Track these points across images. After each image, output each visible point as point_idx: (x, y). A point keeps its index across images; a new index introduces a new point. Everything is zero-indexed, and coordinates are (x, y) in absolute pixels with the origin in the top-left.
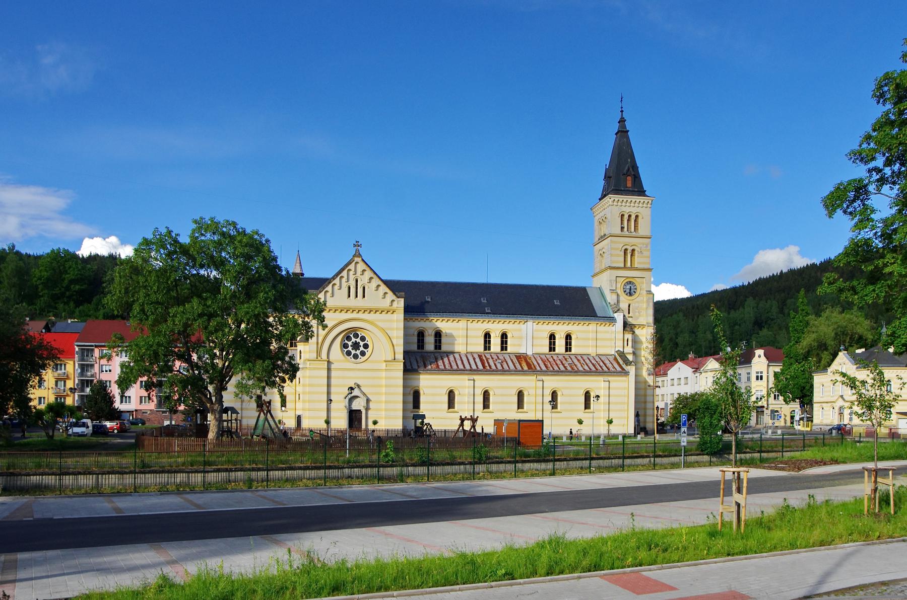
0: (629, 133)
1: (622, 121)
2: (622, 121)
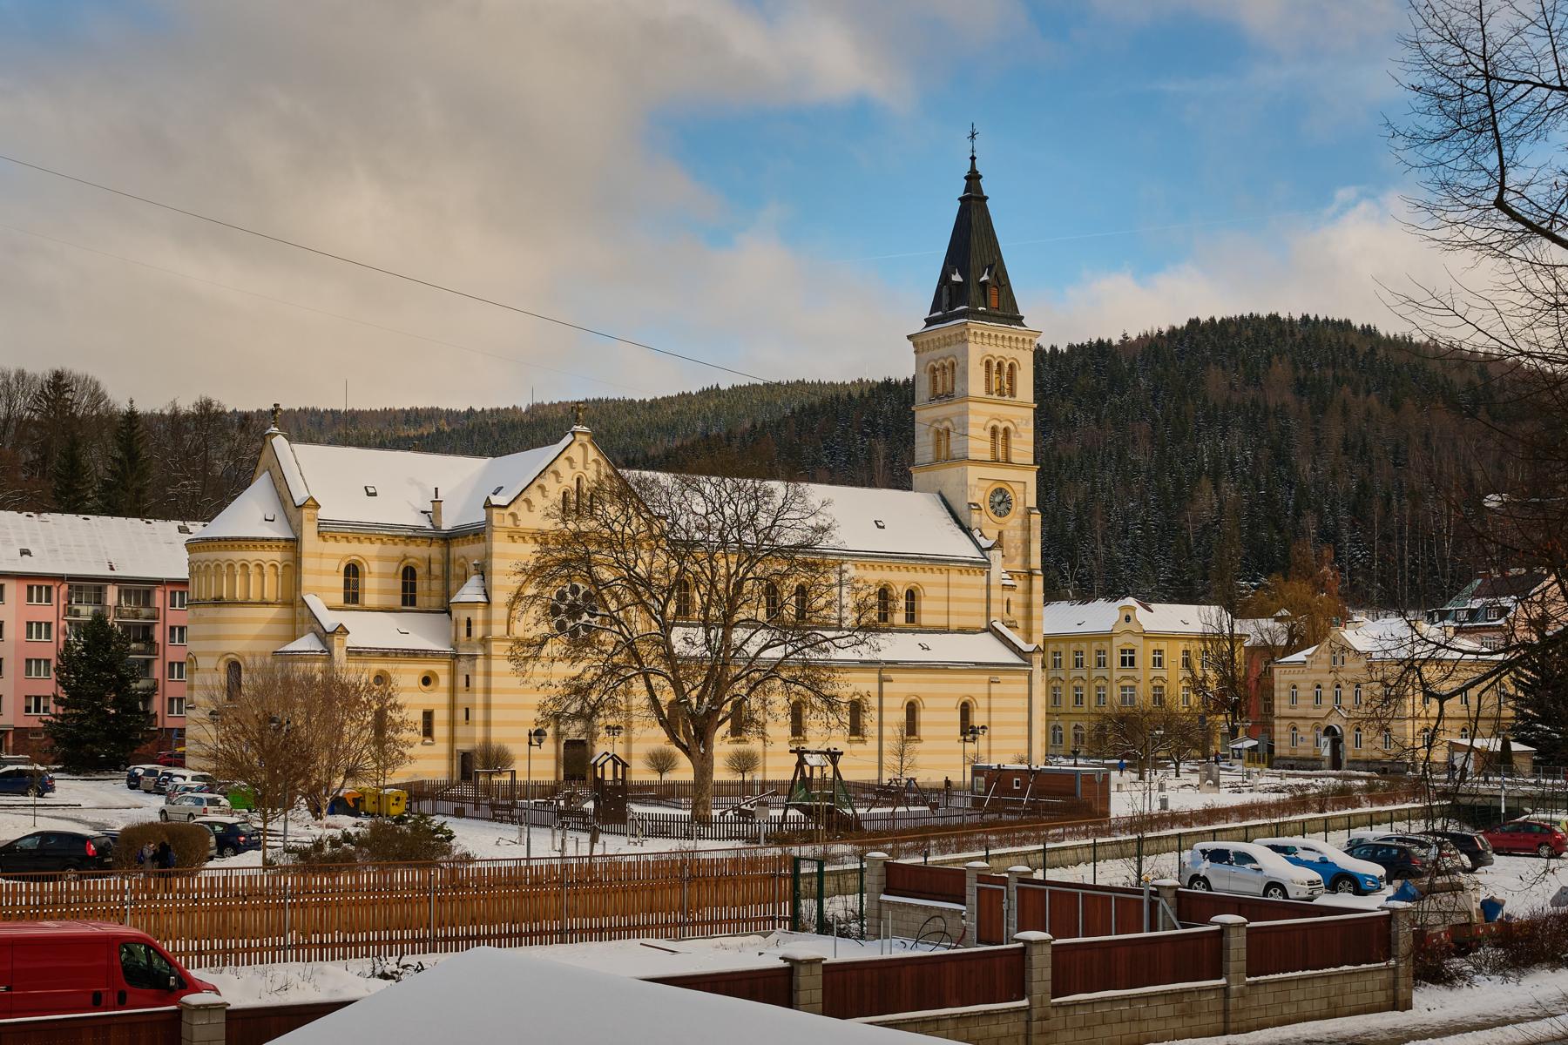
0: (988, 202)
1: (973, 178)
2: (973, 178)
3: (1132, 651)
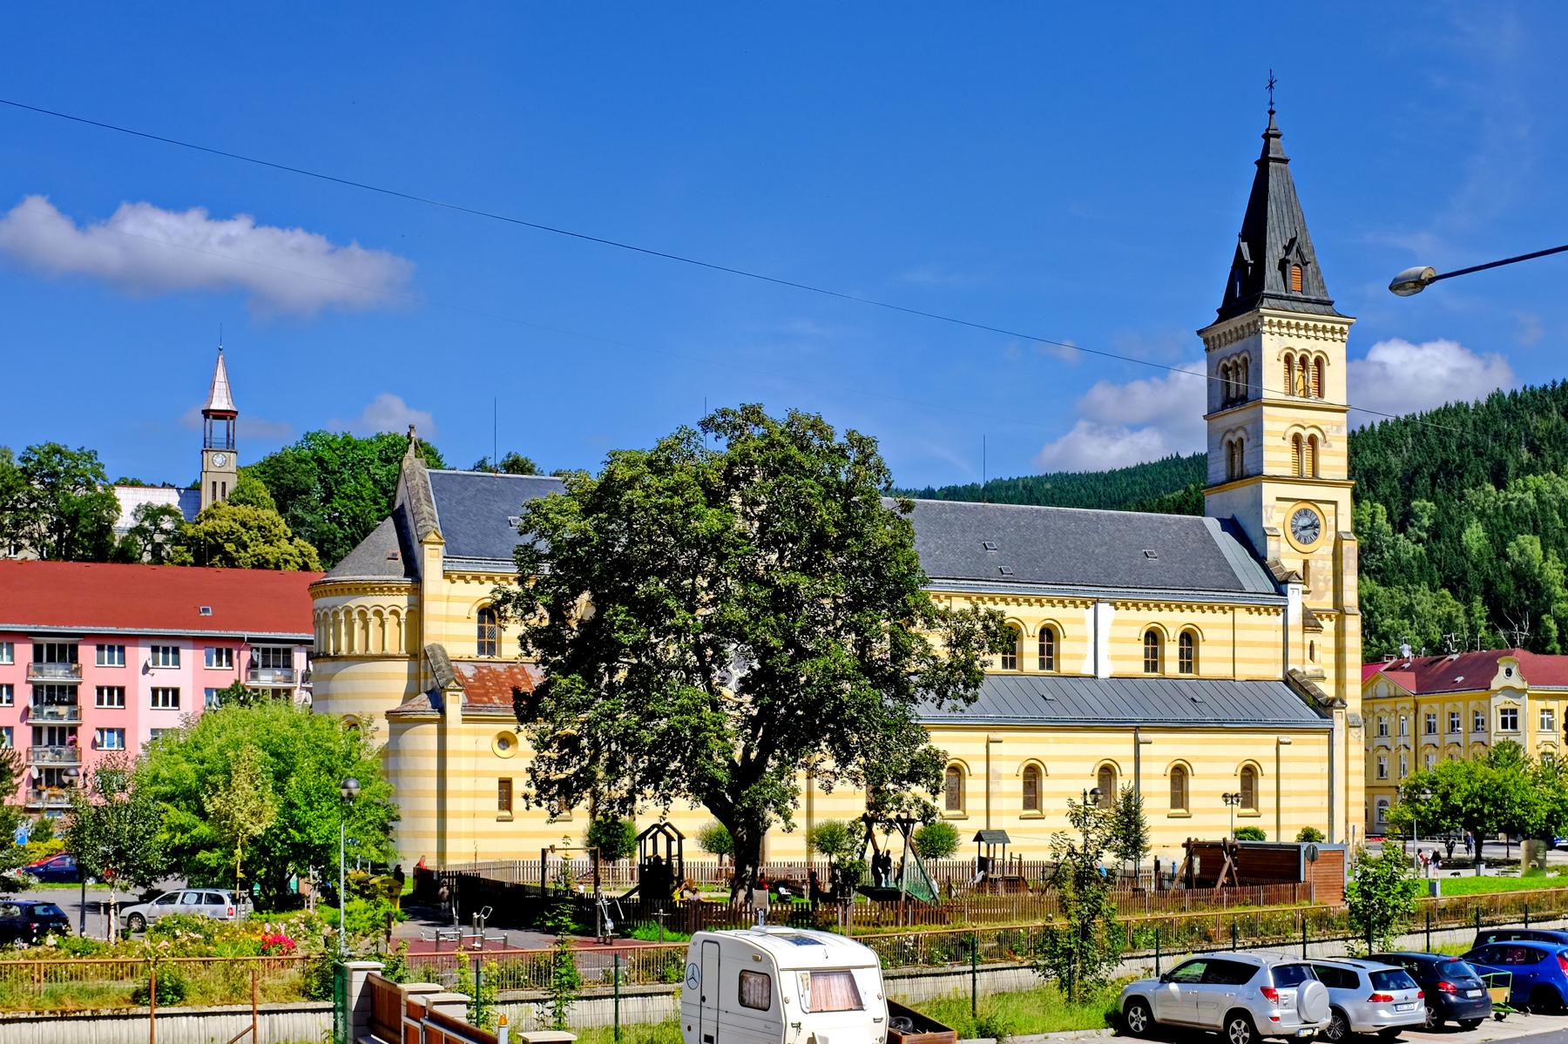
3: (1514, 711)
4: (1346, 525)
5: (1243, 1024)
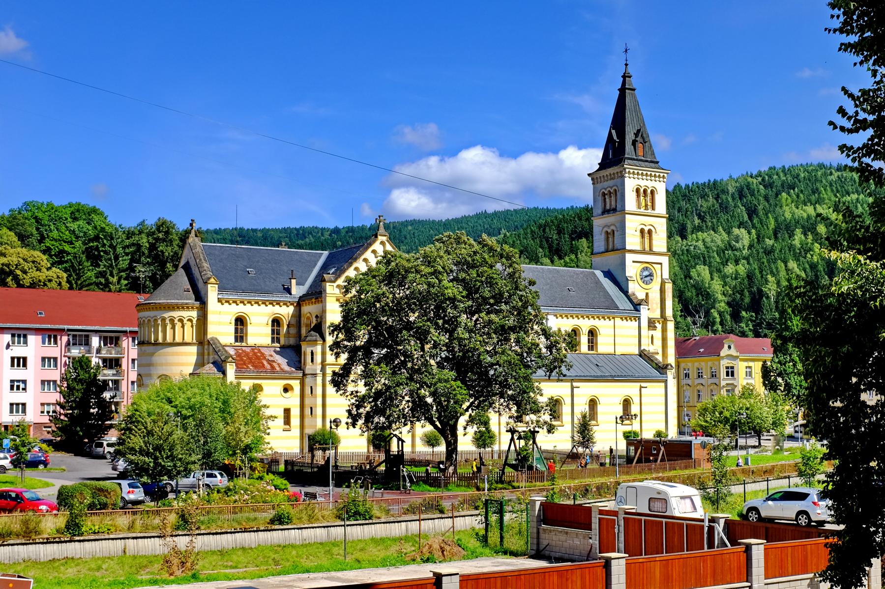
3: (732, 368)
4: (666, 275)
5: (805, 516)
